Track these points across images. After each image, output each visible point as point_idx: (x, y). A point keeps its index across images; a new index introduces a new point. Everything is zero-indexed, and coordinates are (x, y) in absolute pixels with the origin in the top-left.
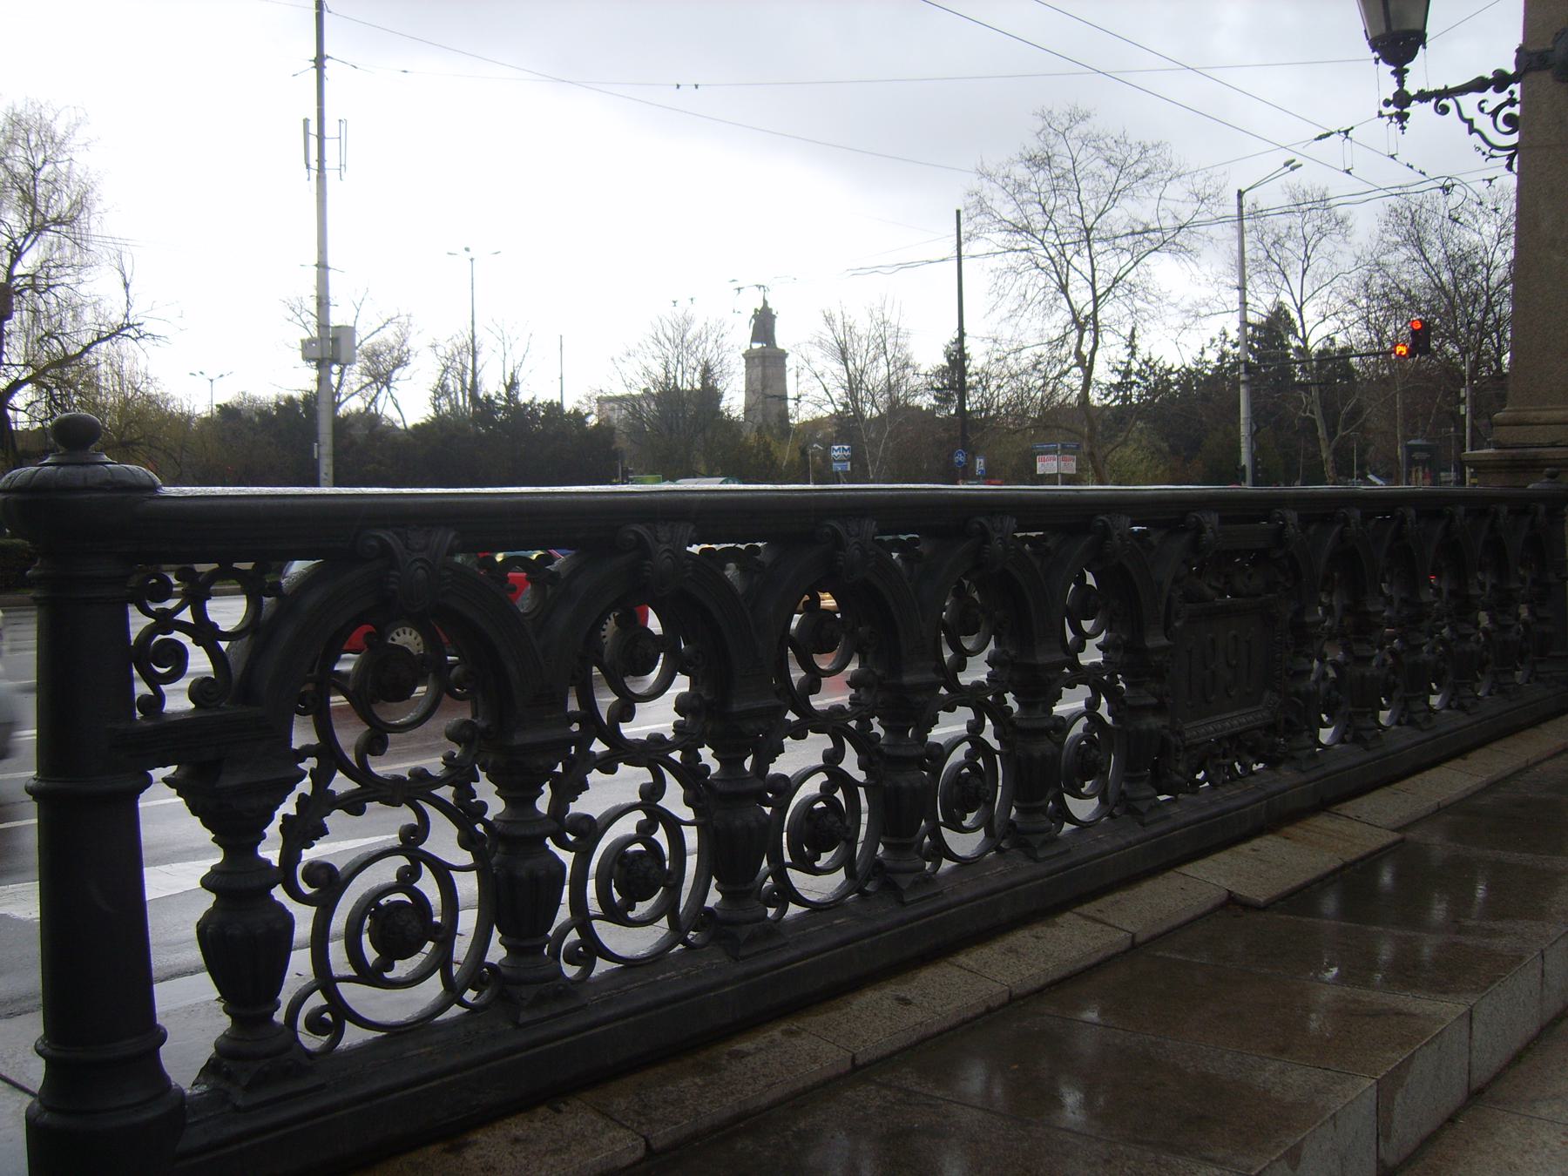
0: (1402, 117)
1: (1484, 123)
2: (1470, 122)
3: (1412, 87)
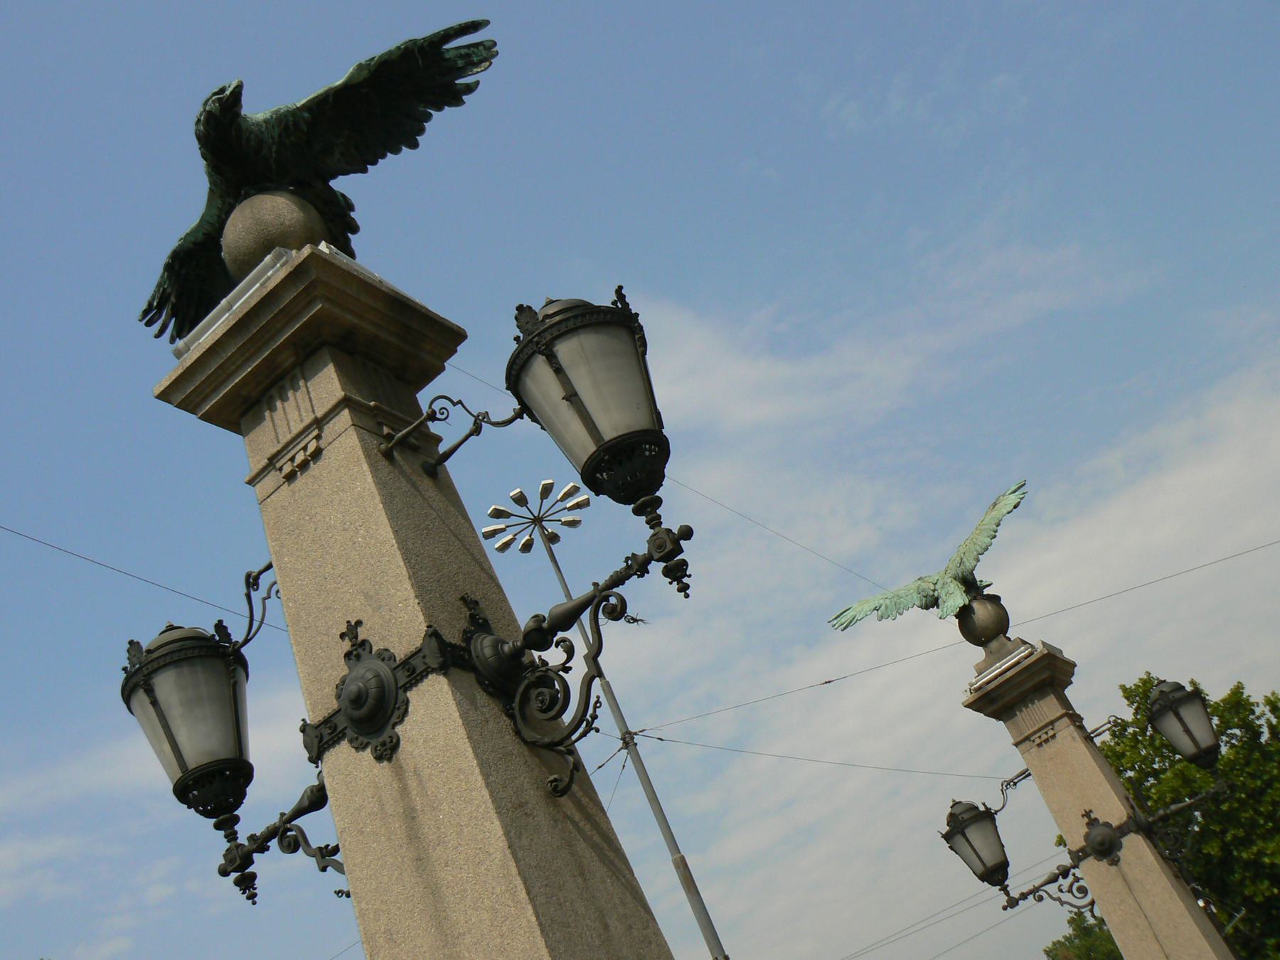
0: (247, 883)
1: (1066, 897)
2: (1059, 899)
3: (1015, 894)
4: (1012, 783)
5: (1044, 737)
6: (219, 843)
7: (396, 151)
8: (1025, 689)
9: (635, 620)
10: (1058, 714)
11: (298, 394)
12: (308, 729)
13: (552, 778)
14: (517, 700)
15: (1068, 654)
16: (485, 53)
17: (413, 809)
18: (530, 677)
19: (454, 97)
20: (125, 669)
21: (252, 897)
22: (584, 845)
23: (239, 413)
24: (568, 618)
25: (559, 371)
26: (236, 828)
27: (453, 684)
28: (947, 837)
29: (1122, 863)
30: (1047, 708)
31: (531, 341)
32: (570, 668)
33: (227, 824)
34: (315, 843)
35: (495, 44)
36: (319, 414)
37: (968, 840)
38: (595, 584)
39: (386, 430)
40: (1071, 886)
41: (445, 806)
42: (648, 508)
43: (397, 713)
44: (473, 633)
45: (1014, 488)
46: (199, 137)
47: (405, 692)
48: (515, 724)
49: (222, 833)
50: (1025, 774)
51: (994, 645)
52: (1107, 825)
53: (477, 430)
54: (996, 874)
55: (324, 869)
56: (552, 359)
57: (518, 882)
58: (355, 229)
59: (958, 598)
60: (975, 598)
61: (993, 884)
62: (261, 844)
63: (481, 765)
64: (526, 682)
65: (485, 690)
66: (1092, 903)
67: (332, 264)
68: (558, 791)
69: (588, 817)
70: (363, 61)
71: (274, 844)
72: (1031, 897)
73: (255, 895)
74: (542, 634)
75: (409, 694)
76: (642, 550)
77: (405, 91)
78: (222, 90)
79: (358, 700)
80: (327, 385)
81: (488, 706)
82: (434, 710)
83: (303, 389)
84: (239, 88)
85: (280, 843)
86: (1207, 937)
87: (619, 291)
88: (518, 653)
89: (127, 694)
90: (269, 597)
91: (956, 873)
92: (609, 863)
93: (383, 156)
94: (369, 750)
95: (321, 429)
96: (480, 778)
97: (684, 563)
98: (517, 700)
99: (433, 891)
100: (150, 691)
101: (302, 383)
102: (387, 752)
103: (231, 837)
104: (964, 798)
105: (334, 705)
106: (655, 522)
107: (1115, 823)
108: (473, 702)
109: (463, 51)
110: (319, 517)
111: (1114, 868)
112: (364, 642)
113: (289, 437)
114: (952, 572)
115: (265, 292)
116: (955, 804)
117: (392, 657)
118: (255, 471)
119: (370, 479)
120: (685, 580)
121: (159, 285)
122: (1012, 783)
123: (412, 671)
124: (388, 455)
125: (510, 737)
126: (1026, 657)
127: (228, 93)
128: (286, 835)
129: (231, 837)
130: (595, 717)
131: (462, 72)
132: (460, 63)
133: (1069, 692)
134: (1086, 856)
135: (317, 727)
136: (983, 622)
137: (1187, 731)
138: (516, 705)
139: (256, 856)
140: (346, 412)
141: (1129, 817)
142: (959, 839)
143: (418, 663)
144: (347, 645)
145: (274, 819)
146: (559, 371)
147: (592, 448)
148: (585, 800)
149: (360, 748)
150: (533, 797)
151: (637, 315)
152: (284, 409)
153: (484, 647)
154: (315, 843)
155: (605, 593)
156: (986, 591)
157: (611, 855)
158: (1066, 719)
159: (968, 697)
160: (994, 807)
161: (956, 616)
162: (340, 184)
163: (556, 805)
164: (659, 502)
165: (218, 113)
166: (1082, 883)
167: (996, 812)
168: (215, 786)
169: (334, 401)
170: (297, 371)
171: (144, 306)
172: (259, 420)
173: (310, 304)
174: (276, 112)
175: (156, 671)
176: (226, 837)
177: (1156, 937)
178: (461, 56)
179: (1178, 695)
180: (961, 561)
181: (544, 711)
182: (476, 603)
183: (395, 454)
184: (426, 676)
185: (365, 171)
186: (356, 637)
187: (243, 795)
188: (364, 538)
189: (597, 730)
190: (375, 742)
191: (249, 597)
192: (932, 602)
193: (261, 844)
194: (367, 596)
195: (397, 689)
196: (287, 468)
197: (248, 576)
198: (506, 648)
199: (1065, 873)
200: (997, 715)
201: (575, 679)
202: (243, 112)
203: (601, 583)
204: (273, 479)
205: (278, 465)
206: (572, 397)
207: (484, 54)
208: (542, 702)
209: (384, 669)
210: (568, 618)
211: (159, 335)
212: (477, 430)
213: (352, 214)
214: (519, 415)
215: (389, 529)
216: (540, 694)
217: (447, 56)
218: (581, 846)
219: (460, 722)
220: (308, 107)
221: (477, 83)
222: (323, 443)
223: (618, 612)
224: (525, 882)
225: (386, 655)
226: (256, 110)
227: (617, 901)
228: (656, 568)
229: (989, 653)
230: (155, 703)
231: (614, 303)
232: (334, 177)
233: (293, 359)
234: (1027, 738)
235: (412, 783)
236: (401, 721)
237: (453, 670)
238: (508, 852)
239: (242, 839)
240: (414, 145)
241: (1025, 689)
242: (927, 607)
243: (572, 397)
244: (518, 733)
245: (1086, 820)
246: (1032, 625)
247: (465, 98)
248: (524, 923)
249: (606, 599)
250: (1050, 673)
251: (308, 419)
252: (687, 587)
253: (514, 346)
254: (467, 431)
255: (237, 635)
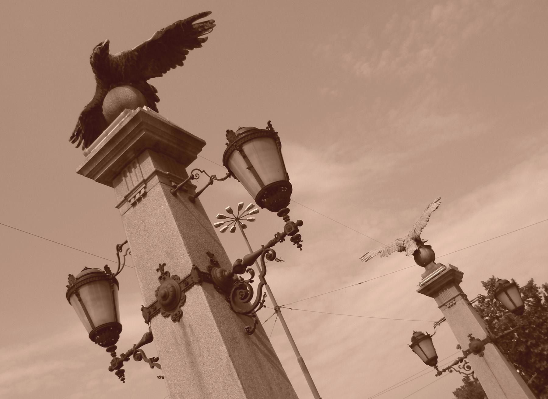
0: (121, 374)
1: (462, 370)
2: (459, 371)
3: (440, 369)
4: (438, 323)
5: (451, 304)
6: (109, 357)
7: (174, 67)
8: (443, 284)
9: (280, 260)
10: (457, 294)
11: (136, 170)
12: (144, 309)
13: (246, 327)
14: (231, 294)
15: (460, 269)
16: (210, 25)
17: (189, 342)
18: (236, 285)
19: (197, 44)
20: (67, 286)
21: (123, 380)
22: (261, 355)
23: (112, 178)
24: (251, 260)
25: (245, 157)
26: (116, 351)
27: (204, 289)
28: (412, 347)
29: (485, 355)
30: (452, 292)
31: (233, 145)
32: (253, 281)
33: (112, 349)
34: (149, 356)
35: (214, 21)
36: (145, 178)
37: (420, 348)
38: (263, 246)
39: (173, 184)
40: (464, 366)
41: (202, 340)
42: (284, 213)
43: (181, 302)
44: (212, 267)
45: (436, 200)
46: (92, 64)
47: (184, 293)
48: (231, 305)
49: (110, 353)
50: (443, 320)
51: (429, 266)
52: (478, 340)
53: (211, 183)
54: (432, 361)
55: (152, 367)
56: (242, 152)
57: (234, 371)
58: (158, 100)
59: (413, 247)
60: (421, 247)
61: (431, 365)
62: (126, 357)
63: (218, 322)
64: (235, 287)
65: (218, 291)
66: (473, 373)
67: (149, 115)
68: (249, 332)
69: (262, 343)
70: (159, 30)
71: (131, 357)
72: (447, 371)
73: (124, 379)
74: (241, 267)
75: (186, 294)
76: (282, 231)
77: (177, 42)
78: (101, 44)
79: (165, 297)
80: (148, 166)
81: (219, 298)
82: (197, 300)
83: (138, 168)
84: (108, 43)
85: (134, 357)
86: (521, 385)
88: (231, 275)
91: (416, 362)
92: (271, 362)
93: (169, 70)
94: (170, 317)
95: (146, 184)
96: (217, 328)
97: (300, 236)
98: (231, 294)
99: (199, 375)
100: (78, 295)
101: (137, 165)
102: (178, 318)
103: (114, 355)
104: (418, 331)
105: (155, 299)
106: (287, 219)
107: (482, 339)
108: (213, 296)
109: (201, 25)
110: (146, 221)
111: (481, 358)
112: (167, 272)
113: (133, 188)
114: (411, 236)
115: (121, 127)
116: (415, 333)
117: (179, 278)
118: (119, 203)
119: (167, 204)
120: (300, 243)
121: (77, 126)
122: (438, 323)
123: (187, 284)
124: (174, 194)
125: (228, 310)
126: (443, 271)
127: (103, 45)
128: (136, 353)
129: (114, 355)
130: (264, 301)
131: (201, 33)
132: (200, 30)
133: (461, 285)
134: (470, 353)
135: (148, 308)
136: (424, 257)
137: (511, 300)
138: (231, 297)
139: (124, 363)
140: (156, 178)
141: (488, 336)
142: (417, 347)
143: (189, 280)
144: (159, 274)
145: (131, 347)
146: (245, 157)
147: (260, 189)
148: (261, 336)
149: (166, 316)
150: (239, 335)
151: (277, 133)
152: (130, 176)
153: (217, 273)
154: (149, 356)
155: (267, 249)
156: (425, 244)
157: (272, 358)
158: (460, 297)
159: (419, 288)
160: (431, 333)
161: (413, 255)
162: (151, 82)
163: (249, 338)
164: (288, 211)
165: (99, 53)
166: (468, 364)
167: (432, 336)
168: (106, 334)
169: (151, 172)
170: (136, 160)
171: (71, 135)
172: (120, 181)
173: (140, 132)
174: (123, 53)
175: (80, 287)
177: (500, 386)
178: (200, 27)
179: (506, 285)
180: (415, 232)
181: (243, 299)
182: (213, 255)
183: (178, 194)
184: (193, 286)
185: (161, 76)
186: (163, 270)
187: (118, 337)
188: (165, 229)
189: (265, 307)
190: (172, 314)
191: (118, 255)
192: (403, 249)
193: (126, 357)
194: (167, 253)
195: (181, 292)
196: (133, 201)
197: (118, 246)
198: (226, 273)
199: (461, 360)
200: (431, 295)
201: (255, 286)
202: (110, 53)
203: (265, 244)
204: (126, 205)
205: (129, 200)
206: (251, 168)
207: (210, 25)
208: (242, 295)
209: (175, 283)
210: (251, 260)
211: (77, 147)
212: (211, 183)
213: (157, 94)
214: (228, 176)
215: (175, 225)
216: (240, 292)
217: (194, 27)
218: (260, 355)
219: (208, 305)
220: (137, 50)
221: (207, 38)
222: (147, 190)
223: (272, 257)
224: (237, 370)
225: (176, 278)
226: (115, 52)
227: (275, 378)
228: (288, 238)
229: (427, 270)
230: (80, 300)
231: (267, 128)
232: (149, 79)
233: (134, 155)
234: (444, 305)
235: (188, 331)
236: (183, 305)
237: (204, 283)
238: (229, 358)
239: (118, 356)
240: (182, 64)
241: (443, 284)
242: (401, 251)
243: (251, 168)
244: (232, 308)
245: (469, 338)
246: (444, 258)
247: (202, 44)
248: (237, 388)
249: (267, 251)
250: (453, 277)
251: (141, 180)
252: (301, 246)
253: (226, 147)
254: (207, 183)
255: (114, 271)
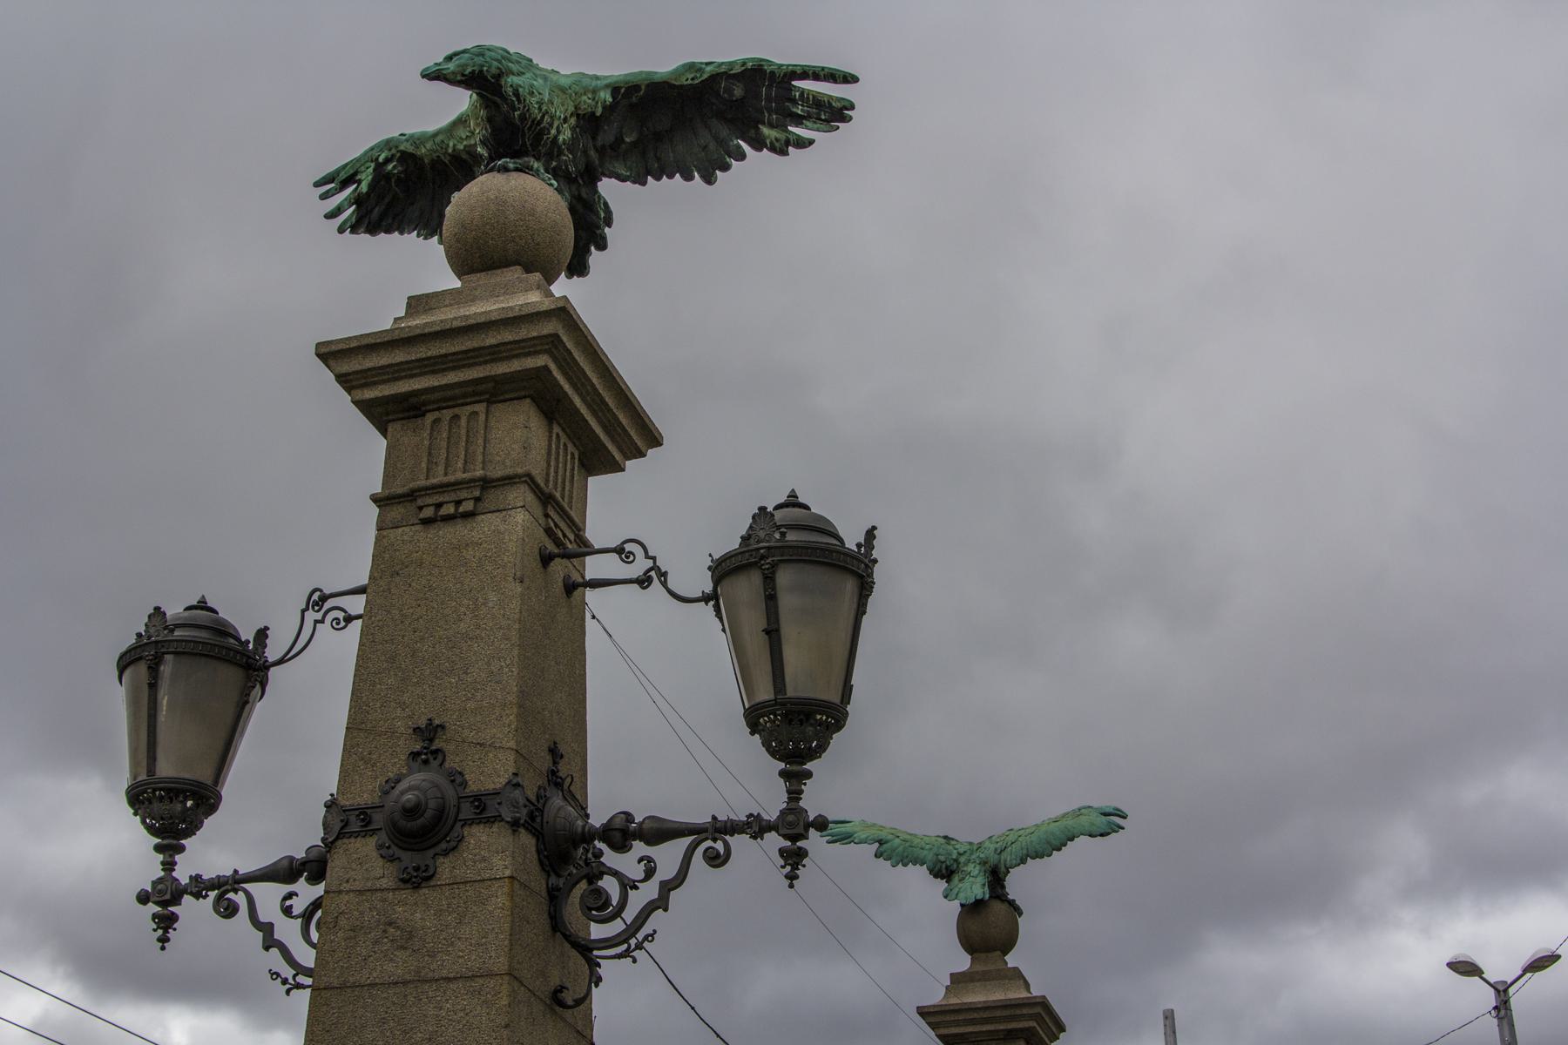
0: (166, 922)
16: (834, 114)
24: (660, 832)
26: (177, 858)
49: (161, 857)
62: (199, 887)
74: (621, 833)
76: (772, 815)
87: (871, 534)
88: (588, 836)
89: (126, 662)
90: (322, 621)
103: (169, 866)
129: (169, 866)
139: (187, 899)
176: (163, 863)
186: (431, 740)
201: (638, 900)
205: (420, 502)
213: (607, 230)
214: (705, 599)
221: (811, 142)
228: (774, 841)
239: (182, 874)
240: (709, 179)
